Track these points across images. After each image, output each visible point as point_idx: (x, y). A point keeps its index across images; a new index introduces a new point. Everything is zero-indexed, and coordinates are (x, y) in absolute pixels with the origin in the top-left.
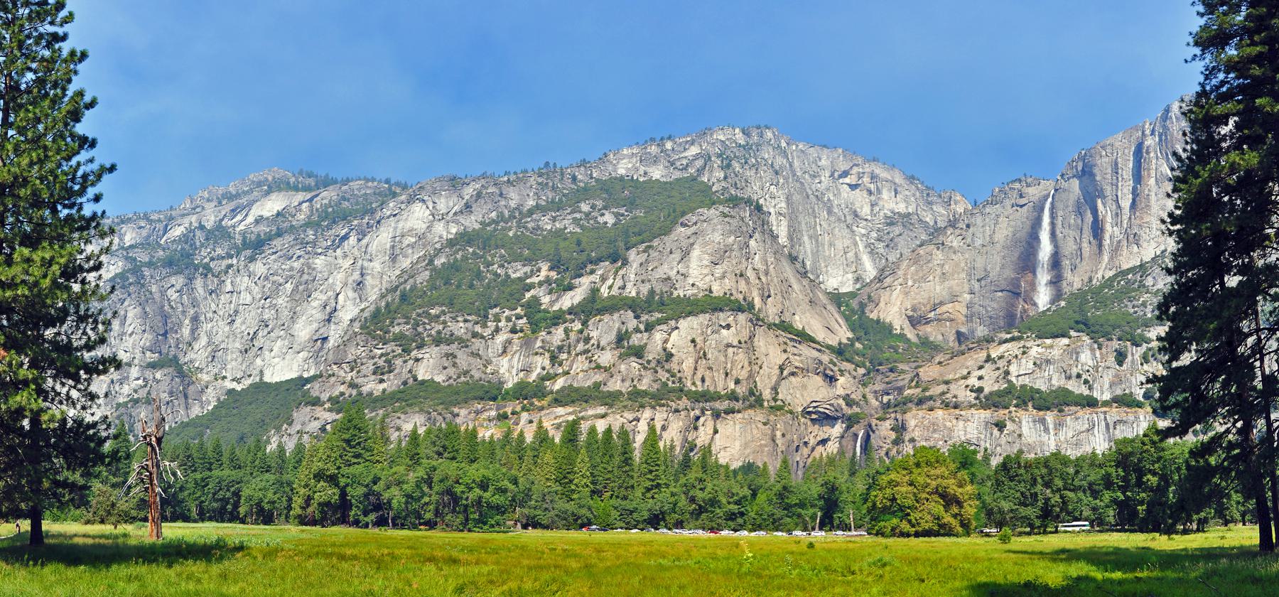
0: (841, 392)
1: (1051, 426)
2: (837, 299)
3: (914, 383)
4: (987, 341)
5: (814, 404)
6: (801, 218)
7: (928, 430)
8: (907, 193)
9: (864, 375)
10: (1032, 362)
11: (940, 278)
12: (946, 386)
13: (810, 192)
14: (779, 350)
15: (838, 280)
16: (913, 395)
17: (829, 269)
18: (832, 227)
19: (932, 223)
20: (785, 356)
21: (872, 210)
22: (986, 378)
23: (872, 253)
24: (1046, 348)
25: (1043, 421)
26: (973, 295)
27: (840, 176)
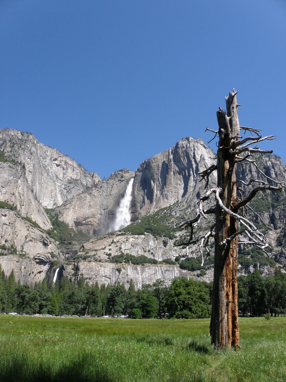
0: (50, 251)
1: (140, 271)
2: (47, 211)
3: (81, 250)
4: (112, 235)
5: (38, 255)
6: (37, 175)
7: (89, 270)
8: (77, 171)
9: (58, 244)
10: (130, 244)
11: (89, 207)
12: (96, 252)
13: (41, 165)
14: (26, 229)
15: (48, 203)
16: (82, 255)
17: (44, 198)
18: (48, 180)
19: (85, 185)
20: (28, 232)
21: (63, 176)
22: (112, 250)
23: (61, 194)
24: (136, 239)
25: (136, 269)
26: (101, 216)
27: (54, 160)
